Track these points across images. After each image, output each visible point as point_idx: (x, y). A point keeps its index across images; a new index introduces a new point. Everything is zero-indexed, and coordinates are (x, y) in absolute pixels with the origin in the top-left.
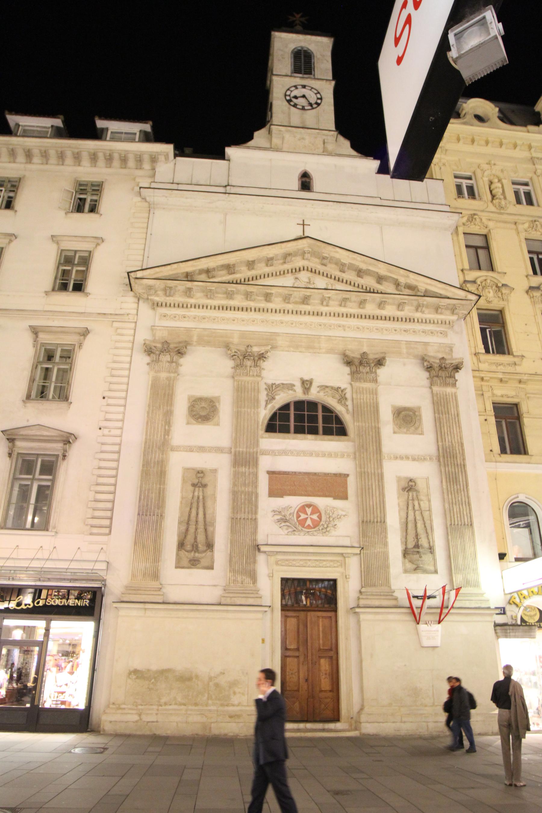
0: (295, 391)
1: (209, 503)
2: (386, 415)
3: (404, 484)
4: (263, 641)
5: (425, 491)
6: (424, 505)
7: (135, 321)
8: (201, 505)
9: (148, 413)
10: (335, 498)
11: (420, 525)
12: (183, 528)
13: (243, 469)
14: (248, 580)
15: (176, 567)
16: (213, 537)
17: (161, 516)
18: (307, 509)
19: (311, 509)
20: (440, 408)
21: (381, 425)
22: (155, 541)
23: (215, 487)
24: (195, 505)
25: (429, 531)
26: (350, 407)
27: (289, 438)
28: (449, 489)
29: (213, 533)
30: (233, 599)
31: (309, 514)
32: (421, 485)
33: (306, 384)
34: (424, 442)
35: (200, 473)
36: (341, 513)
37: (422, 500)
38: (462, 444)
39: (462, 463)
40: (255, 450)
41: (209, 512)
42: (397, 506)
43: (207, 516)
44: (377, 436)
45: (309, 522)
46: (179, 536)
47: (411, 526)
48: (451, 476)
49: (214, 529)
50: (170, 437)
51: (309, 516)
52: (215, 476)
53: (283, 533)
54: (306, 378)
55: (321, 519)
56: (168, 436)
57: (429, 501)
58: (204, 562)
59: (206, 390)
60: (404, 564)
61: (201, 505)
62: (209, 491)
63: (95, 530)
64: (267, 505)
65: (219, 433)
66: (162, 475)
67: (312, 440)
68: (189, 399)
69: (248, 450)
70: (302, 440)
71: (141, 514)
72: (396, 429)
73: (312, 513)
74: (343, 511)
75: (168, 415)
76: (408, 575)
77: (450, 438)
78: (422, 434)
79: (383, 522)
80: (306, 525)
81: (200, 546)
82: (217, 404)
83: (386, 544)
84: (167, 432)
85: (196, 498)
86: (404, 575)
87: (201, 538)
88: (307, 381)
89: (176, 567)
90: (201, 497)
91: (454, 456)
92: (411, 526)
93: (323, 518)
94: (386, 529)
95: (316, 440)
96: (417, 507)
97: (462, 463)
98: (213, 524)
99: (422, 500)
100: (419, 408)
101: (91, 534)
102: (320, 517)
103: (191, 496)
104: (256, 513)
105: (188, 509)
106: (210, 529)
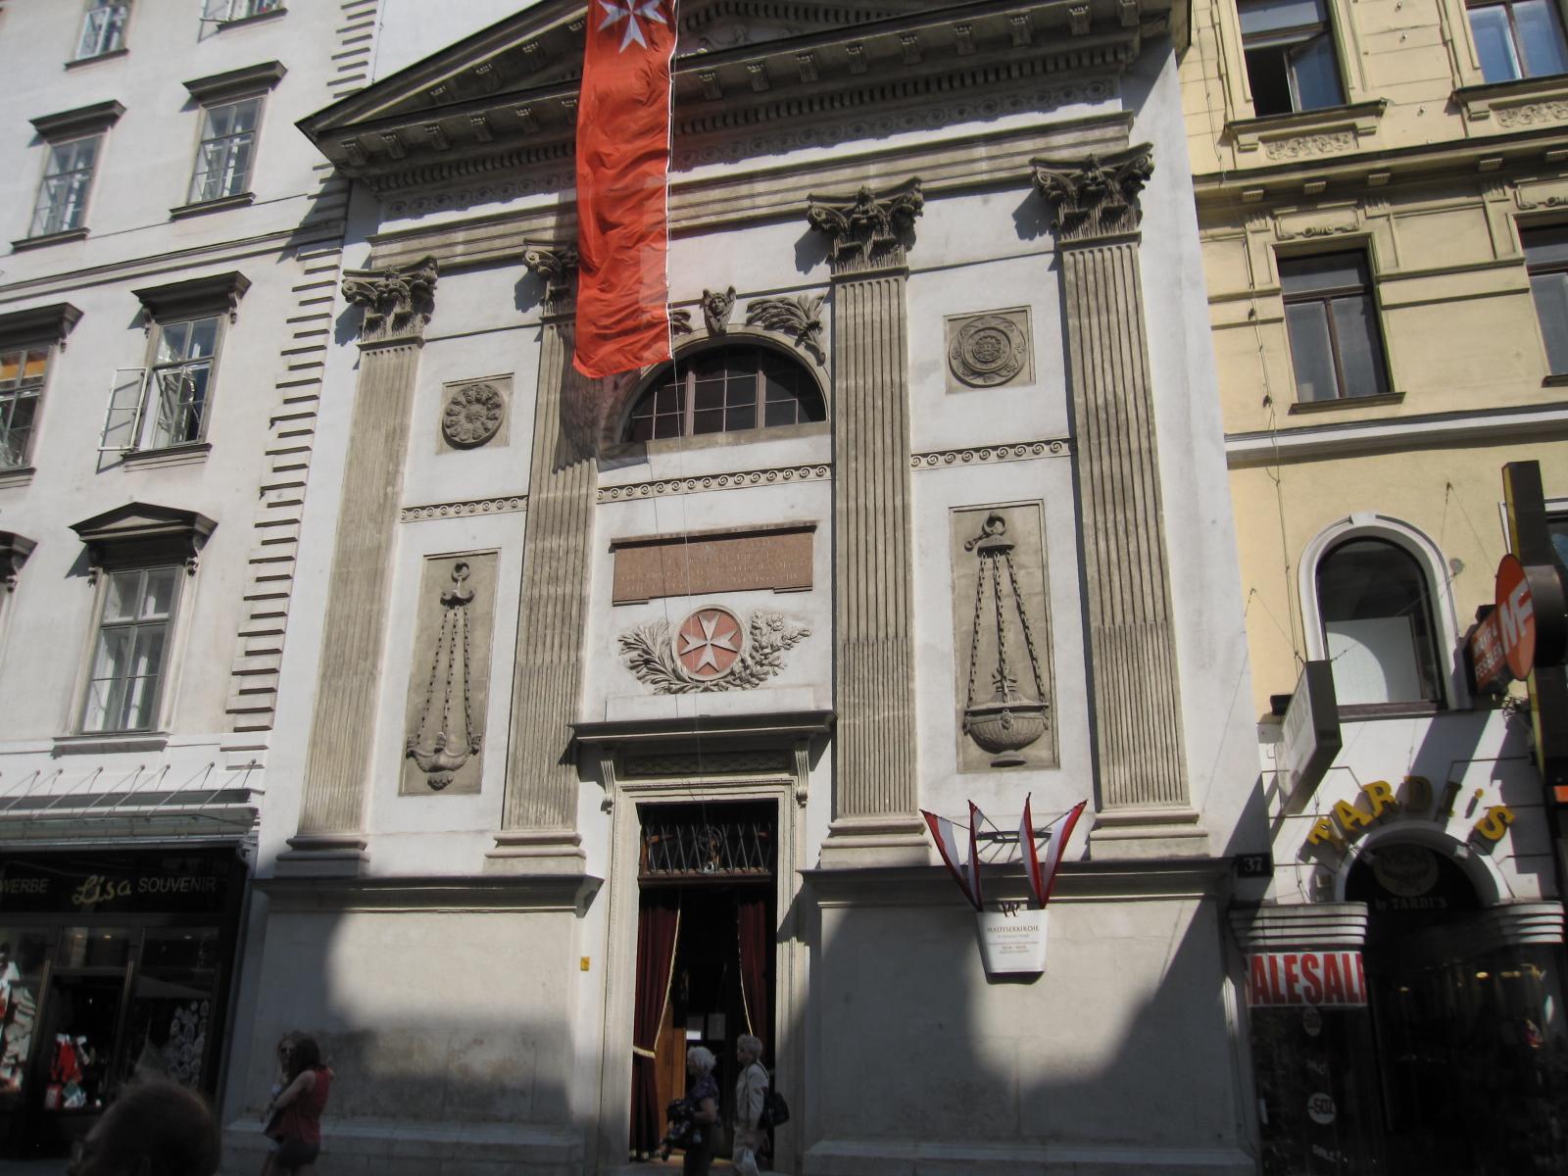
0: (689, 330)
1: (478, 635)
2: (926, 342)
3: (975, 524)
4: (585, 965)
5: (1034, 539)
6: (1027, 580)
7: (341, 233)
8: (459, 641)
9: (352, 440)
10: (778, 591)
11: (1013, 635)
12: (420, 700)
13: (553, 542)
14: (552, 813)
15: (400, 794)
16: (483, 716)
17: (371, 674)
18: (705, 624)
19: (713, 624)
20: (1083, 302)
21: (910, 377)
22: (355, 734)
23: (493, 594)
24: (446, 643)
25: (1040, 651)
26: (826, 348)
27: (670, 450)
28: (1100, 525)
29: (484, 705)
30: (510, 861)
31: (709, 636)
32: (1020, 524)
33: (714, 305)
34: (1033, 405)
35: (460, 565)
36: (792, 626)
37: (1022, 567)
38: (1147, 393)
39: (1145, 444)
40: (584, 491)
41: (476, 656)
42: (950, 589)
43: (473, 666)
44: (897, 406)
45: (708, 656)
46: (409, 719)
47: (987, 640)
48: (1108, 487)
49: (487, 696)
50: (397, 489)
51: (709, 642)
52: (494, 567)
53: (646, 693)
54: (718, 288)
55: (739, 646)
56: (393, 486)
57: (1044, 567)
58: (457, 777)
59: (476, 362)
60: (960, 748)
61: (459, 641)
62: (477, 607)
63: (244, 721)
64: (604, 627)
65: (509, 463)
66: (376, 577)
67: (728, 444)
68: (444, 394)
69: (567, 493)
70: (702, 448)
71: (329, 674)
72: (955, 383)
73: (717, 633)
74: (796, 617)
75: (396, 436)
76: (969, 776)
77: (1109, 379)
78: (1032, 381)
79: (902, 638)
80: (702, 663)
81: (453, 738)
82: (504, 395)
83: (906, 698)
84: (392, 477)
85: (449, 627)
86: (959, 778)
87: (456, 719)
88: (718, 296)
89: (400, 794)
90: (461, 623)
91: (1122, 429)
92: (987, 640)
93: (747, 643)
94: (908, 656)
95: (737, 443)
96: (1005, 586)
97: (1145, 444)
98: (484, 686)
99: (1022, 567)
100: (1023, 310)
101: (237, 730)
102: (737, 638)
103: (440, 621)
104: (579, 646)
105: (432, 654)
106: (476, 696)
